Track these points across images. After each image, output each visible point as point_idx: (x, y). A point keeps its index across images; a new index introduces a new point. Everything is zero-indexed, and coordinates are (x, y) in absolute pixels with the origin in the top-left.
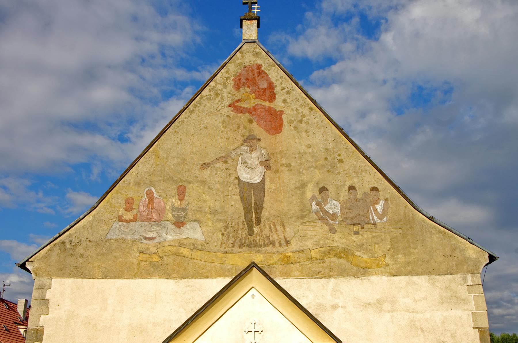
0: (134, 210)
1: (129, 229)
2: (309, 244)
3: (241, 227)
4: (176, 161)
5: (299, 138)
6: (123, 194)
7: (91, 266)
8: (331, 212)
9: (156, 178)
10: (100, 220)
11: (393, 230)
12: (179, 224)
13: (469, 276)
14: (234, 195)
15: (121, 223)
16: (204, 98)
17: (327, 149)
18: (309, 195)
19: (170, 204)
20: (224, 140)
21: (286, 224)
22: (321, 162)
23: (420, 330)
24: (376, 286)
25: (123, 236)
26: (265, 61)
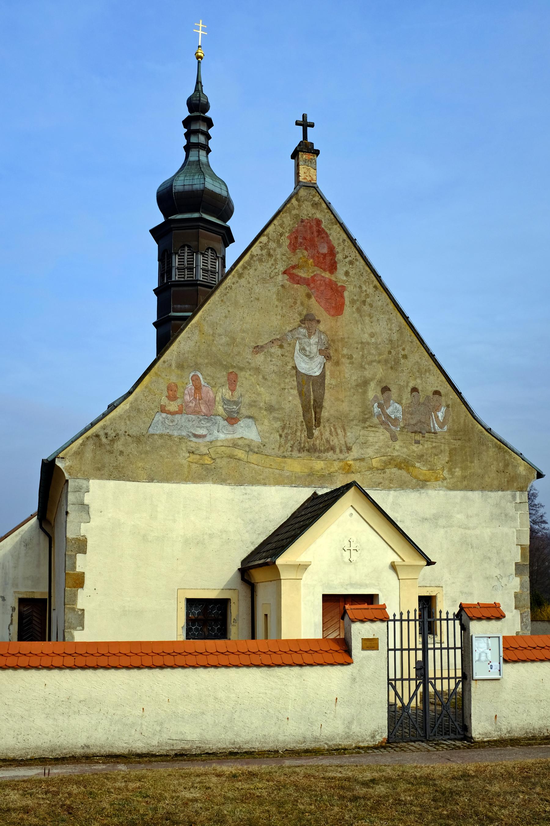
0: (179, 400)
1: (174, 424)
2: (370, 452)
3: (300, 428)
4: (224, 339)
5: (361, 324)
6: (163, 379)
7: (134, 466)
8: (393, 416)
9: (200, 360)
10: (139, 409)
11: (452, 441)
12: (232, 419)
13: (518, 493)
14: (292, 388)
15: (164, 415)
16: (255, 259)
17: (391, 341)
18: (371, 394)
19: (220, 394)
20: (279, 317)
21: (346, 428)
22: (385, 356)
23: (470, 546)
25: (168, 431)
26: (325, 216)
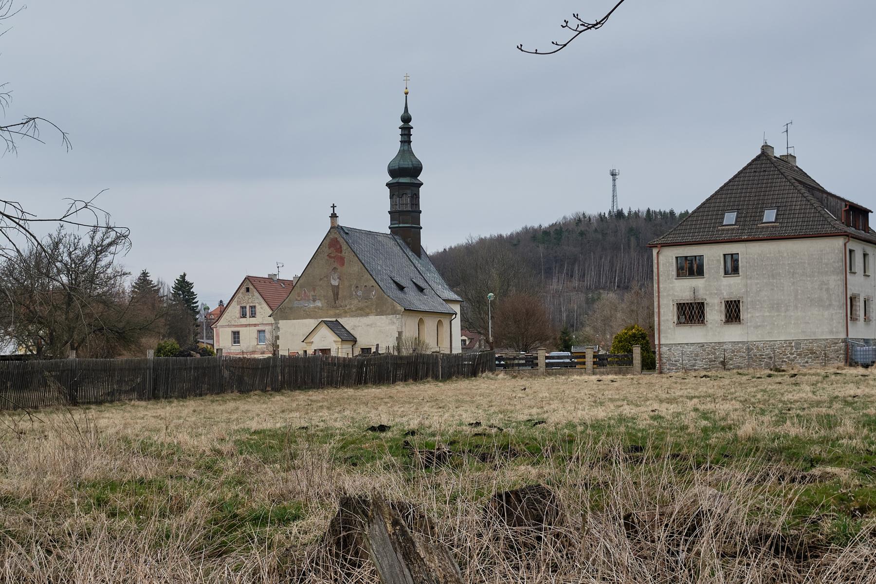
12: (314, 301)
24: (372, 319)
